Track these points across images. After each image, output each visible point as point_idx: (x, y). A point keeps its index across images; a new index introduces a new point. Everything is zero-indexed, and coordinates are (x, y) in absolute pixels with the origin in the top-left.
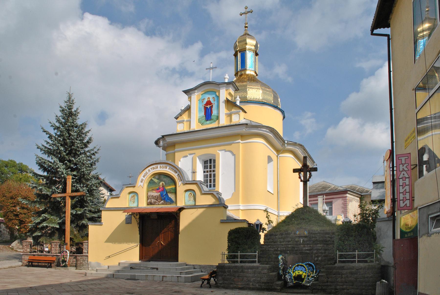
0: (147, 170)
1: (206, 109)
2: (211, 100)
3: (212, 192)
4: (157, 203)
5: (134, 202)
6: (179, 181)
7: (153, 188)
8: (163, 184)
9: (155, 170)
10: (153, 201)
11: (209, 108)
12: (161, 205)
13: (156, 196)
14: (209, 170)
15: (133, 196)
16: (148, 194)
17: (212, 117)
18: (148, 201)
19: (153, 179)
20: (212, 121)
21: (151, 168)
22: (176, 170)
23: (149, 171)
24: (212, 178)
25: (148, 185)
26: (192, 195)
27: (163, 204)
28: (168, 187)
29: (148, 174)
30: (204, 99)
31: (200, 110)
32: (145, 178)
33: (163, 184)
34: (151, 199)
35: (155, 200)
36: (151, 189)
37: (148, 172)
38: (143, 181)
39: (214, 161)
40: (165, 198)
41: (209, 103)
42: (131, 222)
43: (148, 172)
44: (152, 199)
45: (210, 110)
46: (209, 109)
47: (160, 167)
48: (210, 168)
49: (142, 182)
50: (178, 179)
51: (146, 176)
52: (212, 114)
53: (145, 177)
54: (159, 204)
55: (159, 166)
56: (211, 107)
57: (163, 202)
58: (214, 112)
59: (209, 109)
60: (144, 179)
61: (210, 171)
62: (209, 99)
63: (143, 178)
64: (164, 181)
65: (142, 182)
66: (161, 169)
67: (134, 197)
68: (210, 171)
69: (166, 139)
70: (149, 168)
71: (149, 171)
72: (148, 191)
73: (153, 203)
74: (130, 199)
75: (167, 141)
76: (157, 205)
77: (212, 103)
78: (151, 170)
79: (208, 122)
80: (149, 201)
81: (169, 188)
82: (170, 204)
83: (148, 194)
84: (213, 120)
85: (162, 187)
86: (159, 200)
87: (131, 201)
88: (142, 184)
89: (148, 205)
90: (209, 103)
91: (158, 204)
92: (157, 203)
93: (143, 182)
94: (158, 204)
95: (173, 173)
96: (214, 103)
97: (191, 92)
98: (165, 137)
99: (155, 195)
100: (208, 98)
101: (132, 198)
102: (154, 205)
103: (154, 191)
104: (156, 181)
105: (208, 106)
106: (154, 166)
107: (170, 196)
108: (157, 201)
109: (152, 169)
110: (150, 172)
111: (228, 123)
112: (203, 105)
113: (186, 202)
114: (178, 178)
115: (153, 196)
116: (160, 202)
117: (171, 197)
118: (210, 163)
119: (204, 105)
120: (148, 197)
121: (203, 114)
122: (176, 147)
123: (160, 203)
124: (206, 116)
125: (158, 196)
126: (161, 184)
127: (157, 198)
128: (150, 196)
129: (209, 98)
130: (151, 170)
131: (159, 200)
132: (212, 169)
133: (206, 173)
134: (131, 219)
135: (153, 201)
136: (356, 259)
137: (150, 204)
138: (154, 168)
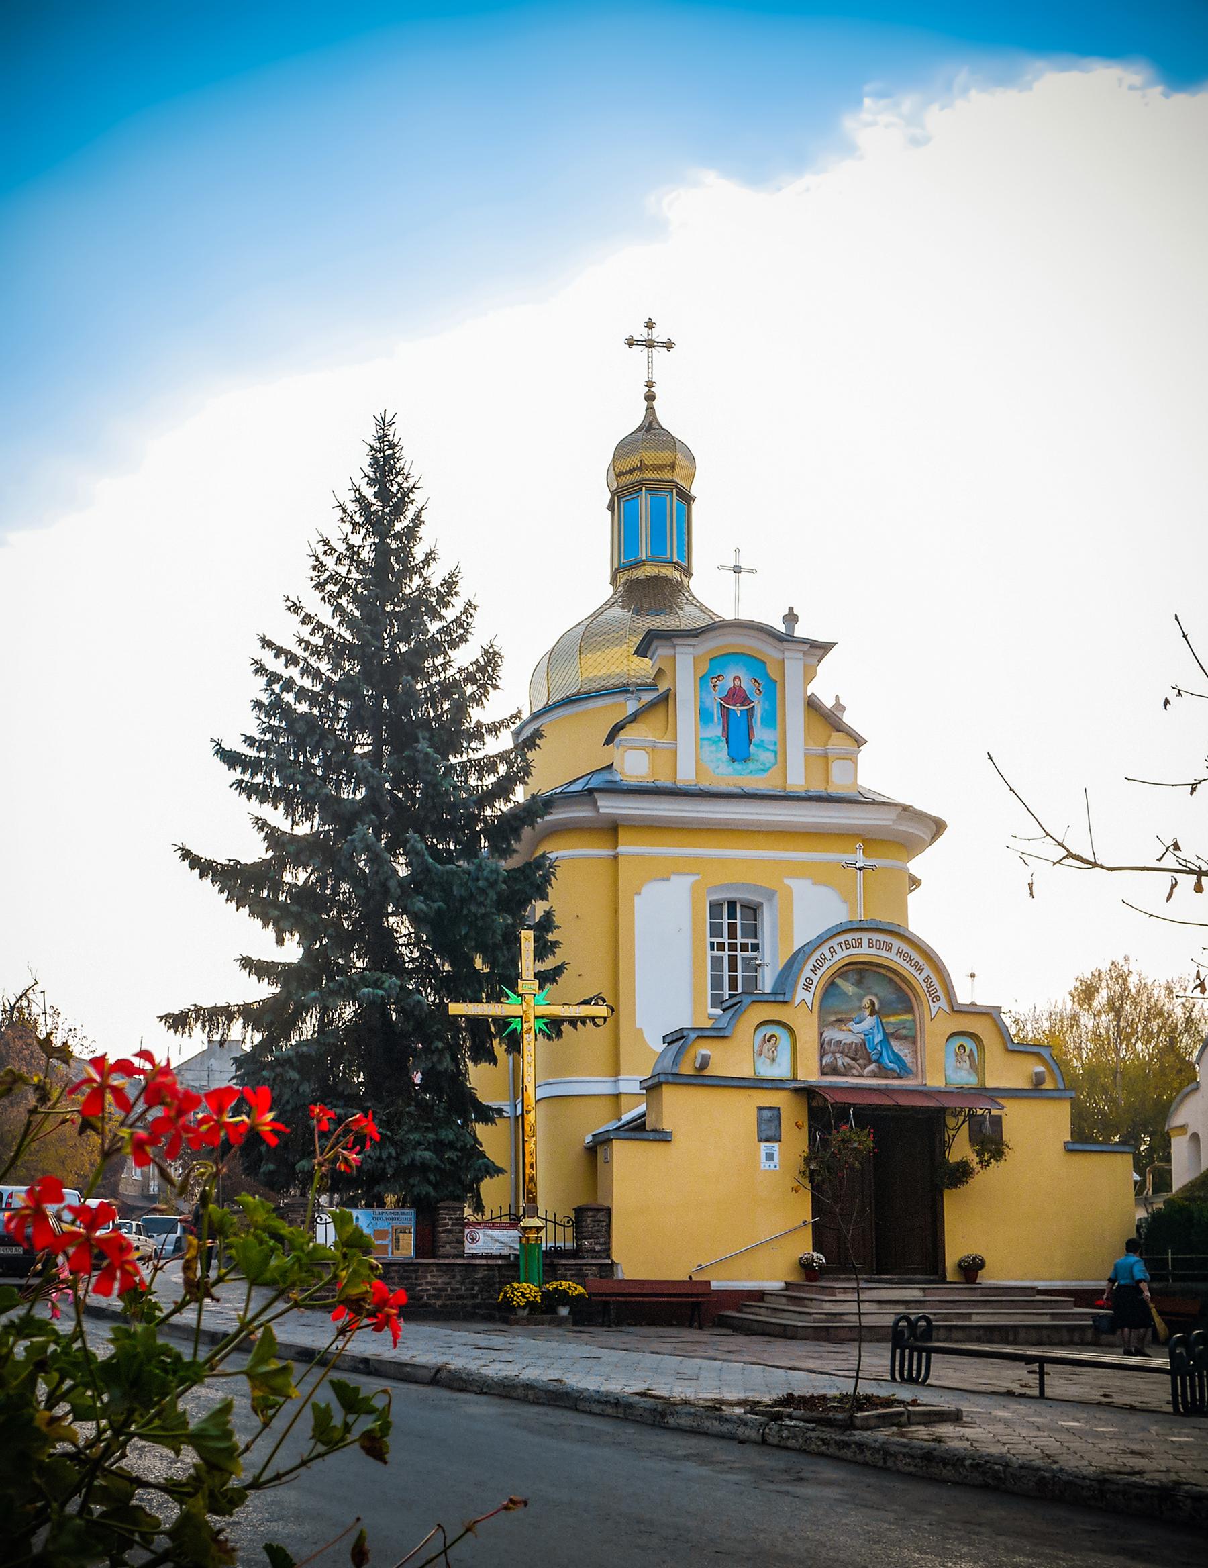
0: (825, 950)
1: (726, 713)
2: (746, 684)
3: (1035, 1050)
4: (855, 1072)
6: (930, 999)
8: (873, 1004)
9: (852, 951)
10: (840, 1062)
14: (726, 940)
15: (772, 1036)
17: (752, 749)
18: (824, 1062)
21: (840, 944)
23: (833, 952)
24: (726, 973)
27: (874, 1075)
28: (889, 1016)
31: (704, 715)
33: (873, 1004)
34: (834, 1053)
35: (847, 1060)
36: (833, 1018)
37: (828, 956)
38: (813, 987)
39: (753, 910)
40: (881, 1054)
43: (828, 956)
44: (838, 1055)
45: (744, 725)
47: (870, 941)
48: (733, 935)
49: (807, 988)
51: (823, 969)
53: (819, 973)
54: (861, 1076)
55: (865, 937)
56: (751, 712)
57: (876, 1070)
60: (815, 979)
61: (733, 947)
64: (876, 995)
65: (807, 988)
66: (873, 951)
67: (772, 1042)
68: (733, 947)
69: (599, 804)
70: (834, 942)
71: (833, 952)
72: (823, 1024)
73: (842, 1069)
75: (601, 810)
78: (837, 949)
80: (827, 1059)
81: (893, 1019)
82: (899, 1077)
83: (824, 1036)
85: (871, 1015)
86: (861, 1061)
88: (808, 997)
89: (823, 1073)
92: (855, 1072)
93: (812, 990)
94: (857, 1074)
95: (912, 969)
97: (677, 641)
98: (596, 795)
99: (849, 1041)
100: (735, 678)
101: (767, 1046)
103: (844, 1028)
104: (848, 988)
105: (738, 709)
106: (848, 937)
109: (843, 946)
110: (836, 958)
111: (817, 788)
114: (926, 989)
115: (840, 1042)
116: (866, 1066)
118: (732, 915)
120: (822, 1045)
121: (717, 730)
122: (622, 836)
126: (866, 1002)
127: (856, 1053)
130: (837, 949)
131: (861, 1061)
132: (739, 940)
133: (716, 953)
135: (841, 1061)
137: (829, 1070)
138: (848, 945)
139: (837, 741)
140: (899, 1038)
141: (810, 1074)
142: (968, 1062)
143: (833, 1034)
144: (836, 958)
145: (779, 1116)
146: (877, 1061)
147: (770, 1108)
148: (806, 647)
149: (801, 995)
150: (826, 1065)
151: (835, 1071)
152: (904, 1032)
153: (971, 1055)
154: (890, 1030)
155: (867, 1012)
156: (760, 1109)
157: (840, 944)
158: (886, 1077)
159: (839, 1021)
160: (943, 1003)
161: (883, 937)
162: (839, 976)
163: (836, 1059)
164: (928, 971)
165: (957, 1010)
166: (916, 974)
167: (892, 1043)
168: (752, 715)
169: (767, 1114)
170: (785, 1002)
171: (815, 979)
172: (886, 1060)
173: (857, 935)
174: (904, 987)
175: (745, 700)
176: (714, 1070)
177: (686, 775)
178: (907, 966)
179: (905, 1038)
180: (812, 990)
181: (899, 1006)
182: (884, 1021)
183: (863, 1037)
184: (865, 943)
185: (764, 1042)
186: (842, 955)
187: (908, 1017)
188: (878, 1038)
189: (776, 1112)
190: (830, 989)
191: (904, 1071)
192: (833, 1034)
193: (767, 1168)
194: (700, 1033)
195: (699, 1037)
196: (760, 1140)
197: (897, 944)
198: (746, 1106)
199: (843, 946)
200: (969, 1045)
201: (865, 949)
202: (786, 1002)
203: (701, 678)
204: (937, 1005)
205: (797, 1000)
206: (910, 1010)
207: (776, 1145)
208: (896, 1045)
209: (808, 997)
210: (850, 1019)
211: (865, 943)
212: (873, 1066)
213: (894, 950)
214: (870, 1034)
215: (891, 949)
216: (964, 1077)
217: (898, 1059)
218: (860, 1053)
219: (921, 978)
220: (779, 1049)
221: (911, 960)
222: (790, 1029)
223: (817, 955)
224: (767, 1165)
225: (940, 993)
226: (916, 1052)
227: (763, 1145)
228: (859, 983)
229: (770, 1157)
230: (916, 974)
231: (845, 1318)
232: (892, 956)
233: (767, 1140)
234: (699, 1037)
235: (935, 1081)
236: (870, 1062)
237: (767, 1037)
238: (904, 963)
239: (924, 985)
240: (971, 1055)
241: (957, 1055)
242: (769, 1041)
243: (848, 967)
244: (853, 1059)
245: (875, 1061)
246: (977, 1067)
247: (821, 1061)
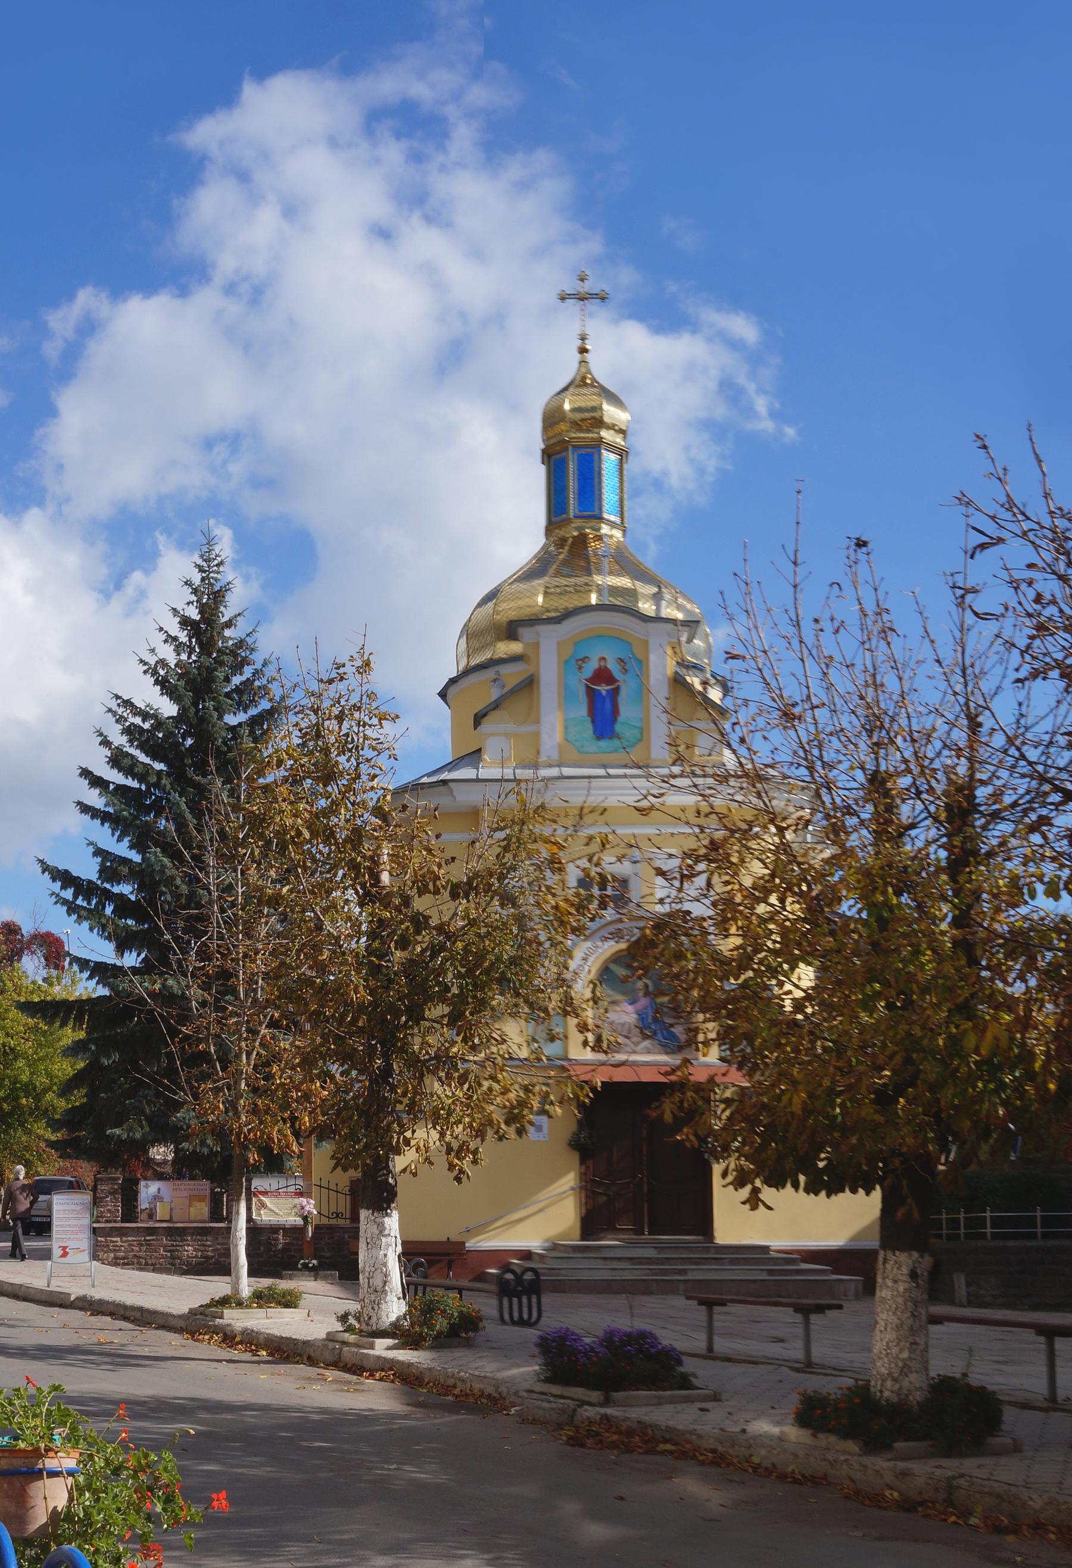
1: (592, 694)
2: (613, 666)
8: (646, 986)
11: (604, 693)
13: (623, 1025)
17: (618, 727)
19: (613, 967)
20: (616, 743)
27: (648, 1052)
30: (585, 659)
33: (646, 986)
41: (603, 675)
45: (608, 704)
52: (619, 719)
54: (634, 1052)
56: (615, 692)
57: (650, 1046)
58: (627, 711)
62: (602, 664)
79: (604, 744)
90: (603, 675)
96: (625, 681)
99: (622, 1021)
103: (618, 1009)
105: (603, 689)
116: (638, 1044)
121: (581, 710)
124: (593, 722)
127: (629, 1031)
129: (604, 659)
131: (635, 1039)
136: (1039, 1230)
155: (641, 994)
193: (536, 1138)
203: (566, 662)
231: (562, 1272)
244: (627, 1037)
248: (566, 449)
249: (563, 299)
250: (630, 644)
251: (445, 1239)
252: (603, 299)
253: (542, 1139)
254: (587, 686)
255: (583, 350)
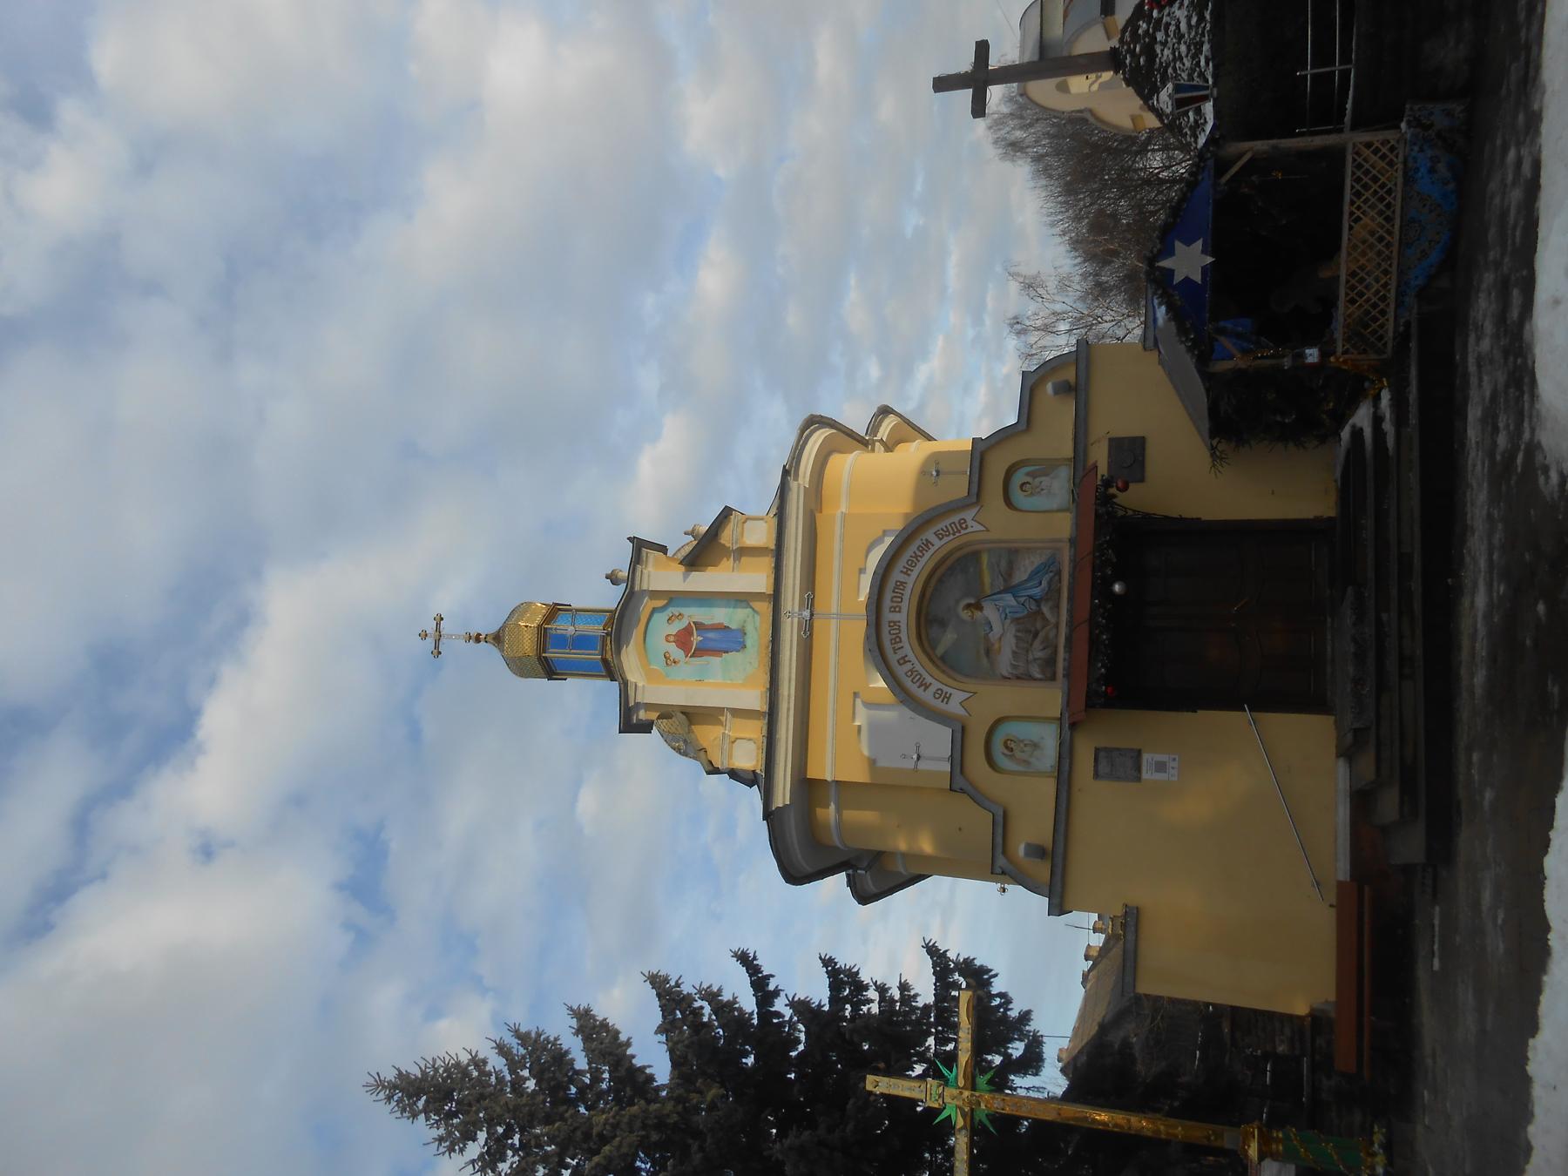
0: (901, 671)
1: (700, 652)
4: (1052, 634)
5: (1035, 746)
6: (963, 532)
7: (982, 652)
8: (968, 606)
9: (904, 636)
10: (1039, 654)
12: (1059, 616)
15: (1007, 747)
16: (1005, 678)
17: (733, 626)
18: (1039, 676)
19: (940, 650)
21: (895, 652)
22: (918, 543)
25: (967, 676)
26: (1028, 483)
27: (1056, 607)
29: (918, 667)
32: (933, 681)
33: (968, 606)
35: (1037, 644)
36: (985, 660)
38: (945, 689)
40: (1030, 597)
41: (683, 639)
42: (1132, 750)
43: (908, 666)
44: (1031, 657)
45: (711, 635)
46: (705, 639)
47: (893, 610)
50: (954, 534)
51: (925, 675)
53: (929, 679)
54: (1057, 626)
55: (888, 616)
56: (699, 626)
59: (705, 639)
62: (672, 639)
63: (932, 689)
64: (957, 602)
65: (947, 698)
66: (905, 605)
67: (1013, 745)
70: (893, 658)
71: (903, 661)
74: (1021, 768)
76: (1057, 635)
77: (686, 624)
78: (900, 654)
81: (987, 579)
82: (1059, 573)
83: (1006, 674)
84: (745, 622)
86: (1039, 625)
87: (1027, 763)
89: (1053, 678)
90: (683, 639)
91: (1054, 631)
93: (950, 690)
95: (927, 555)
99: (1013, 641)
101: (1018, 754)
102: (1056, 647)
103: (997, 646)
104: (948, 638)
105: (696, 639)
107: (1025, 577)
108: (1041, 635)
109: (897, 646)
110: (911, 656)
112: (686, 663)
113: (1055, 506)
114: (952, 537)
115: (1014, 653)
116: (1044, 618)
117: (1029, 571)
119: (686, 657)
120: (1018, 678)
123: (1052, 620)
125: (1018, 631)
126: (965, 615)
127: (1028, 631)
128: (1014, 667)
129: (668, 635)
130: (900, 654)
131: (1039, 625)
134: (1118, 749)
135: (1038, 652)
138: (896, 640)
139: (727, 537)
140: (1009, 574)
141: (1051, 699)
142: (1043, 479)
143: (1004, 661)
144: (911, 656)
145: (1106, 749)
146: (1038, 602)
147: (1096, 760)
148: (639, 567)
149: (954, 707)
150: (1043, 672)
151: (1050, 662)
152: (1003, 564)
153: (1033, 475)
154: (1000, 584)
155: (978, 614)
156: (1097, 775)
157: (895, 652)
158: (1059, 591)
159: (988, 652)
160: (968, 515)
161: (888, 595)
162: (934, 648)
163: (1035, 659)
164: (929, 535)
165: (976, 494)
166: (933, 550)
167: (1014, 584)
168: (702, 624)
169: (1104, 767)
170: (963, 729)
171: (936, 685)
172: (1036, 591)
173: (885, 629)
174: (949, 563)
175: (687, 632)
176: (1043, 834)
177: (755, 699)
178: (923, 561)
179: (1011, 566)
180: (950, 690)
181: (971, 570)
182: (988, 592)
183: (1008, 621)
184: (896, 617)
185: (1012, 757)
186: (909, 647)
187: (985, 559)
188: (1009, 599)
189: (1102, 754)
190: (947, 663)
191: (1051, 566)
192: (1004, 661)
193: (1175, 772)
194: (999, 850)
195: (1004, 852)
196: (1139, 779)
197: (896, 576)
198: (1095, 797)
199: (897, 646)
200: (1019, 477)
201: (901, 617)
202: (963, 729)
204: (970, 523)
205: (961, 711)
206: (976, 555)
207: (1146, 757)
208: (1020, 576)
209: (957, 696)
210: (986, 637)
211: (896, 617)
212: (1045, 609)
213: (902, 578)
214: (1004, 610)
215: (902, 583)
216: (1059, 487)
217: (1035, 573)
218: (1029, 626)
219: (938, 543)
220: (1021, 738)
221: (916, 556)
222: (999, 722)
223: (908, 683)
224: (1172, 771)
225: (956, 518)
226: (1028, 549)
227: (1145, 775)
228: (943, 624)
229: (1161, 767)
230: (933, 550)
232: (910, 581)
233: (1139, 769)
234: (1004, 852)
235: (1063, 526)
236: (1039, 612)
237: (1006, 752)
238: (919, 566)
239: (946, 539)
240: (1033, 475)
241: (1032, 494)
242: (1012, 750)
243: (924, 637)
244: (1036, 635)
245: (1039, 606)
246: (1047, 467)
247: (1035, 680)
248: (546, 658)
249: (440, 653)
250: (654, 608)
251: (1333, 912)
252: (442, 619)
253: (1175, 764)
254: (691, 657)
255: (478, 639)
